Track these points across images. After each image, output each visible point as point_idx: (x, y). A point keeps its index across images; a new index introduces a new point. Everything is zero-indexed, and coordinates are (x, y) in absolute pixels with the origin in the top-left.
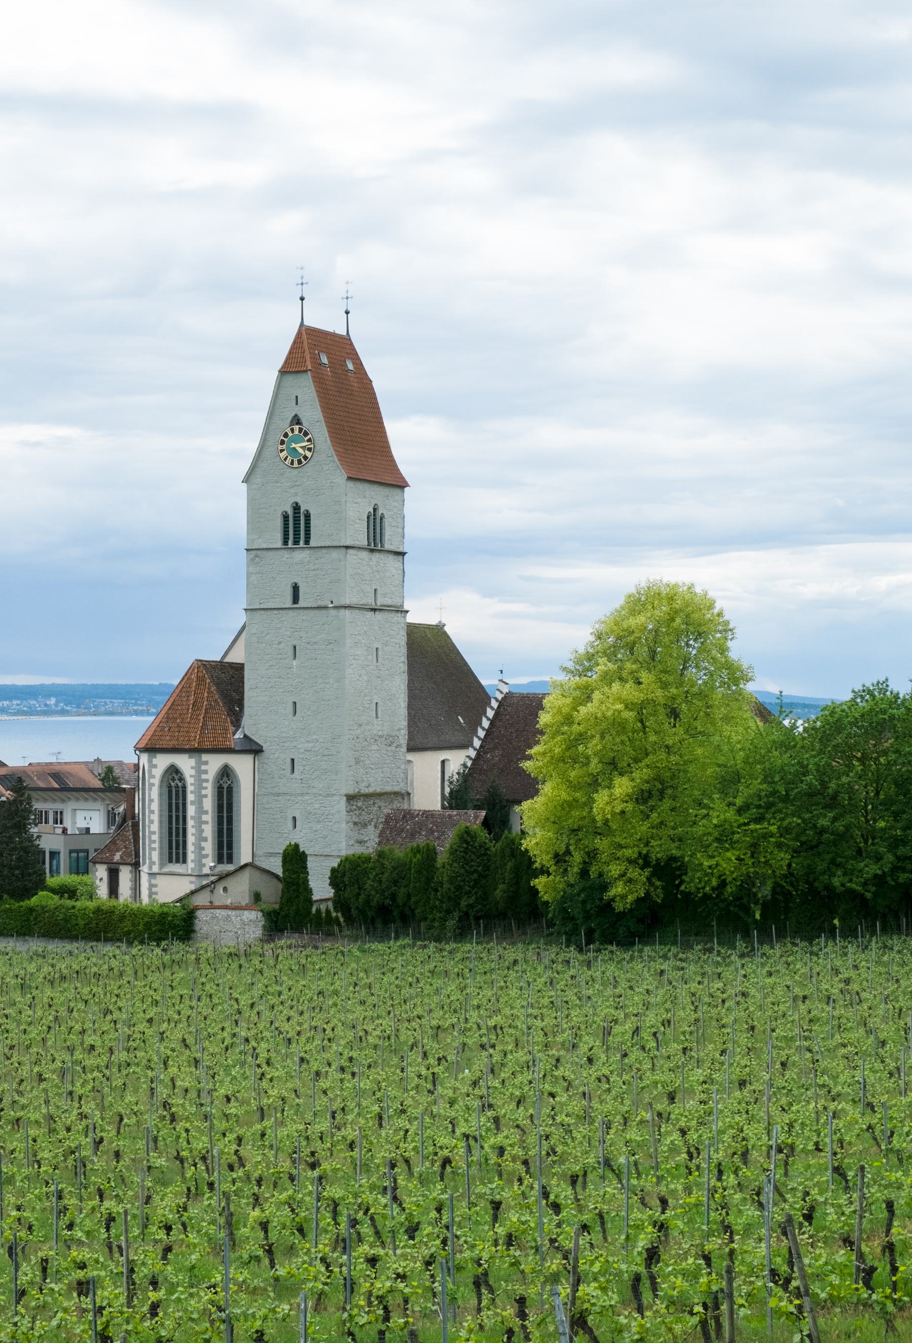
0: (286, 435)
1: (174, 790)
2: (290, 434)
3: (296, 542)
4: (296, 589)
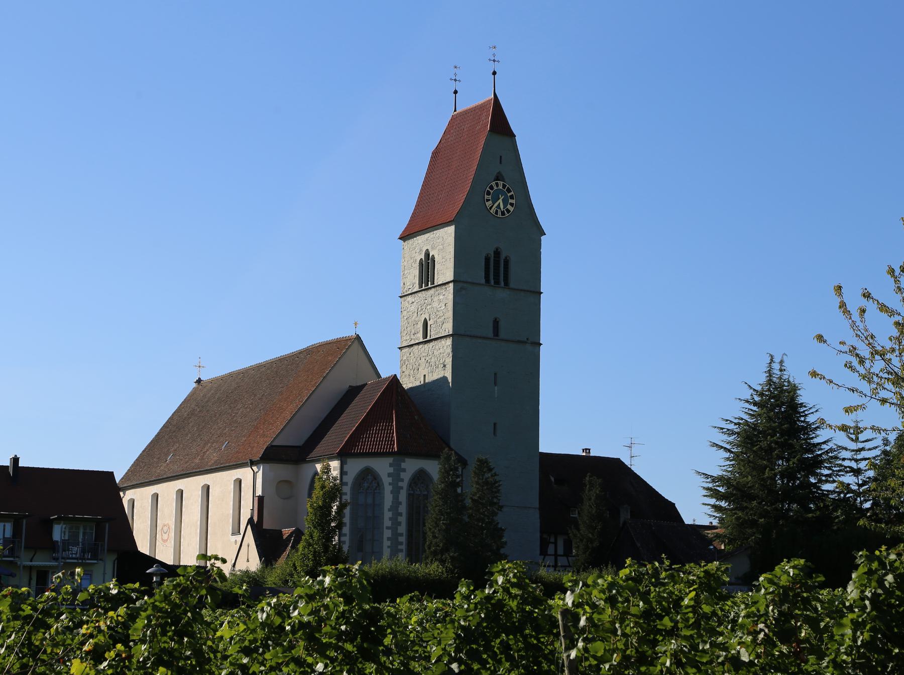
0: (492, 188)
2: (495, 188)
3: (497, 282)
4: (496, 323)
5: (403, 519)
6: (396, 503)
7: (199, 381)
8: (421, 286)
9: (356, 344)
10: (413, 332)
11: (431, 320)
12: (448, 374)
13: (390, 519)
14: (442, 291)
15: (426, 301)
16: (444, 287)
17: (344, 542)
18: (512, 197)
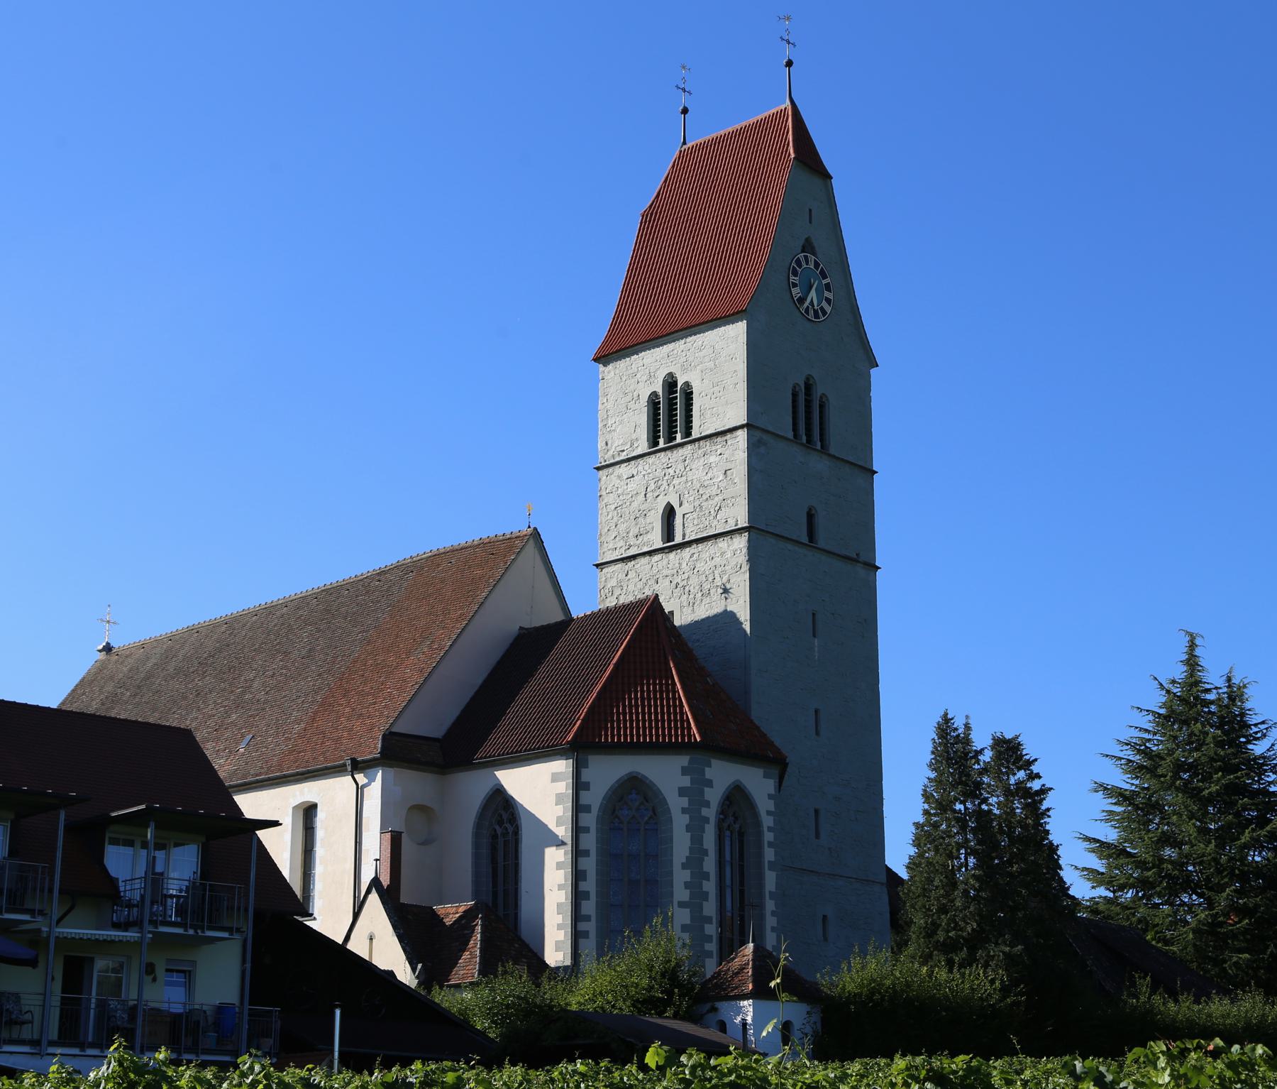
0: (799, 263)
1: (501, 840)
5: (710, 886)
6: (697, 853)
7: (108, 649)
8: (654, 441)
9: (531, 548)
10: (634, 531)
11: (685, 505)
12: (741, 607)
13: (687, 885)
14: (714, 448)
15: (671, 471)
16: (719, 439)
17: (586, 934)
18: (828, 287)
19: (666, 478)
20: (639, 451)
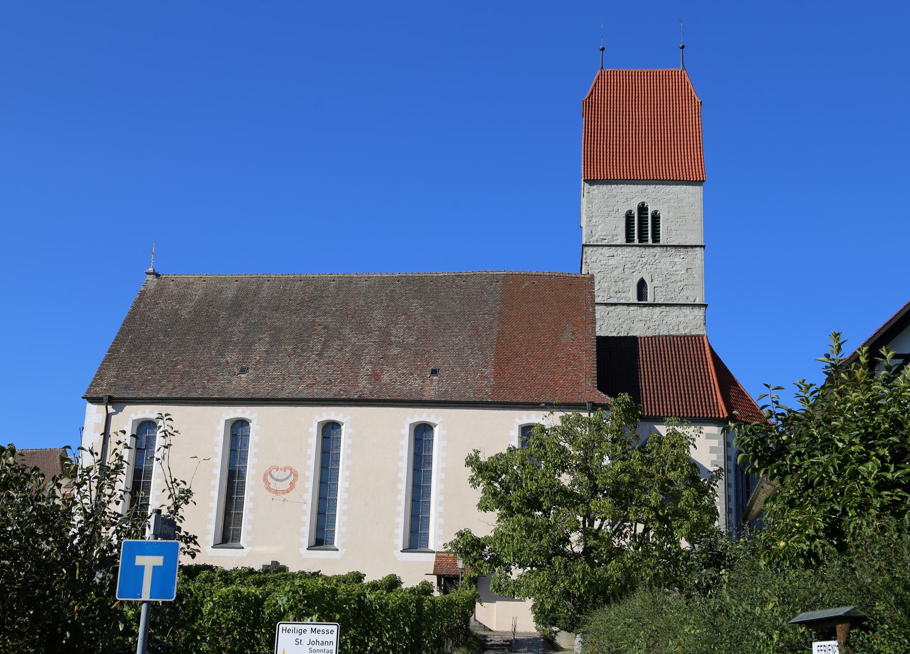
11: (656, 283)
19: (641, 262)
20: (618, 242)
